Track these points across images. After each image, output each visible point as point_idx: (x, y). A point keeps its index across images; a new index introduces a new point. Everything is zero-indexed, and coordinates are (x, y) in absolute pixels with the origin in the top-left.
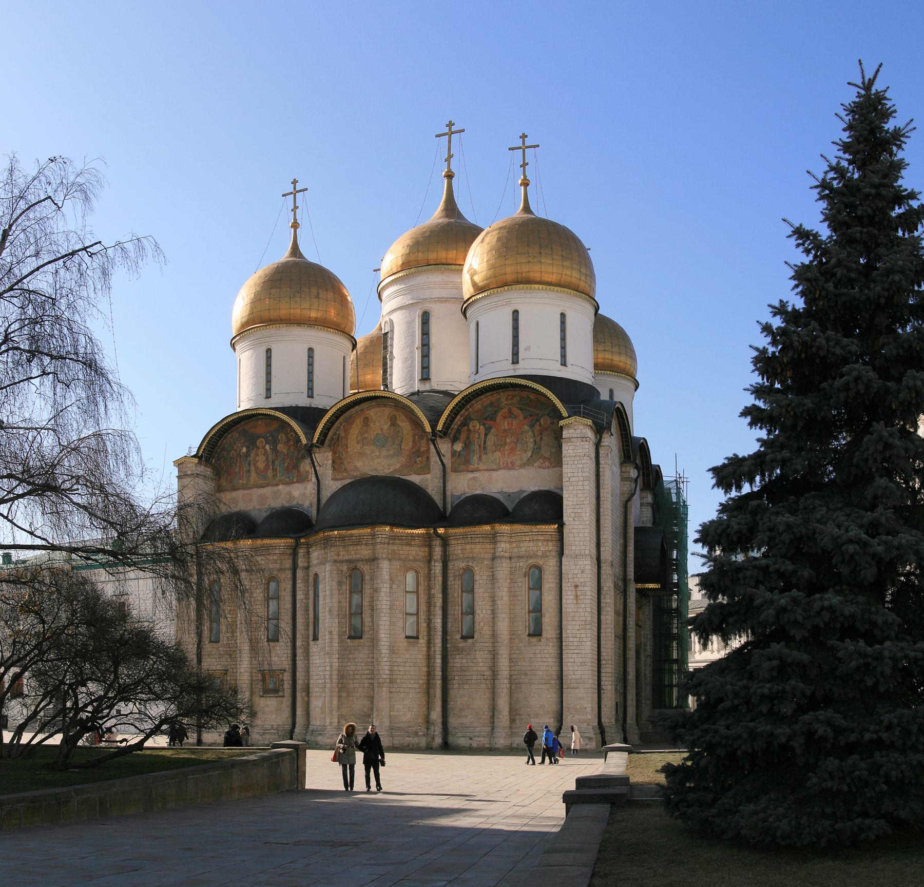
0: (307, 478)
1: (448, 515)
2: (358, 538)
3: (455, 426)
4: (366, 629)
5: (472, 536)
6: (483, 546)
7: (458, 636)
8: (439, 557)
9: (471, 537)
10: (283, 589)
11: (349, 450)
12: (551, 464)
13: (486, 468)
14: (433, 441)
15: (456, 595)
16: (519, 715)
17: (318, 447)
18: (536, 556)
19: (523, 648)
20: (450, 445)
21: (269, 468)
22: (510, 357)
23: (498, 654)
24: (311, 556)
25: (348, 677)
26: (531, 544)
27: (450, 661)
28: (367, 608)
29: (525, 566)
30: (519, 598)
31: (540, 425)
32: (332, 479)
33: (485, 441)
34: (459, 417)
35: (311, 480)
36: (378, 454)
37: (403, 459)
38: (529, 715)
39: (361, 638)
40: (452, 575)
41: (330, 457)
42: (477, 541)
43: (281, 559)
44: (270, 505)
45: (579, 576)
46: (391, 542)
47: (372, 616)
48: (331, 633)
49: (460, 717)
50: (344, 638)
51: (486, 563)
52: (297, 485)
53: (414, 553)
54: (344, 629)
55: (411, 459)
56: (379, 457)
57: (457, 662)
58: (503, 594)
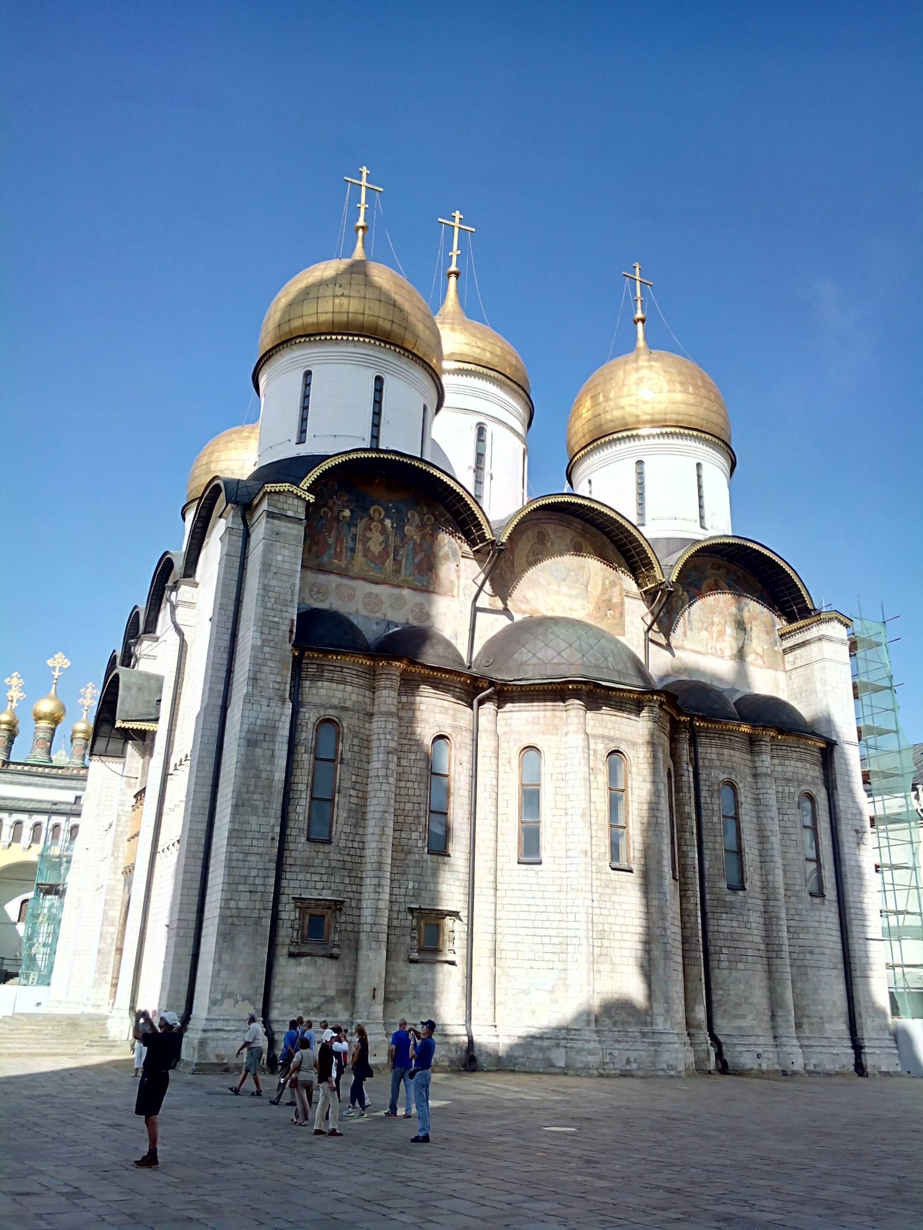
0: (452, 591)
5: (731, 738)
7: (724, 885)
10: (458, 763)
12: (764, 663)
13: (692, 648)
15: (715, 819)
16: (808, 1017)
18: (808, 783)
19: (805, 913)
21: (388, 557)
23: (778, 918)
25: (611, 937)
26: (799, 764)
27: (711, 922)
29: (797, 794)
30: (793, 837)
31: (749, 609)
36: (556, 588)
37: (591, 607)
38: (821, 1018)
40: (707, 788)
44: (385, 615)
49: (737, 1017)
51: (749, 779)
55: (600, 609)
57: (724, 924)
58: (774, 826)
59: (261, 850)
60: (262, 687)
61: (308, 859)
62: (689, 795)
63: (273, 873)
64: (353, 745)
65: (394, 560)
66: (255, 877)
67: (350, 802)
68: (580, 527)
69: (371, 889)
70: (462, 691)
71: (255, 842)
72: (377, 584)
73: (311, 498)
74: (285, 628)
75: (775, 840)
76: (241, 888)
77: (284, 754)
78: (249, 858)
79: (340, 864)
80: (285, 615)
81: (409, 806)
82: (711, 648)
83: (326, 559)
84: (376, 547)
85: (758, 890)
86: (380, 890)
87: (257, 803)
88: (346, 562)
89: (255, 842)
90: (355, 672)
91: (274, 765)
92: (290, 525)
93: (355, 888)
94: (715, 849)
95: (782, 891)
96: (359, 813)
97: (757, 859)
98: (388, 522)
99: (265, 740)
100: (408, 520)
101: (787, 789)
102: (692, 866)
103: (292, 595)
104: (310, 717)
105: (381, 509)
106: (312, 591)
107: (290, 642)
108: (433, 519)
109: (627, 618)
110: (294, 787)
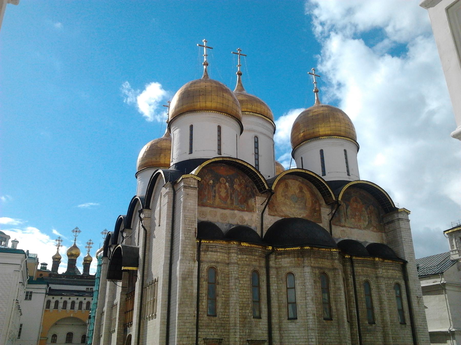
0: (254, 210)
4: (334, 314)
7: (367, 322)
10: (262, 281)
11: (277, 199)
12: (377, 230)
15: (362, 296)
19: (399, 331)
26: (393, 271)
27: (363, 337)
28: (332, 299)
29: (393, 283)
30: (393, 301)
33: (346, 212)
36: (294, 205)
37: (307, 212)
39: (332, 320)
43: (259, 260)
45: (418, 291)
47: (336, 305)
48: (314, 314)
50: (321, 318)
51: (374, 279)
52: (247, 213)
54: (321, 313)
56: (294, 207)
58: (385, 297)
59: (190, 321)
60: (186, 256)
61: (208, 323)
62: (351, 287)
63: (195, 330)
64: (222, 277)
66: (188, 331)
67: (222, 300)
69: (233, 333)
71: (188, 318)
73: (199, 179)
74: (193, 232)
75: (386, 303)
76: (184, 336)
77: (196, 282)
78: (186, 324)
79: (220, 325)
80: (193, 226)
81: (244, 300)
82: (356, 225)
83: (205, 201)
84: (223, 194)
85: (380, 323)
86: (236, 334)
87: (188, 302)
88: (212, 202)
89: (188, 318)
90: (220, 247)
91: (193, 286)
92: (192, 190)
93: (226, 333)
94: (363, 308)
95: (389, 323)
96: (226, 304)
97: (379, 311)
98: (227, 184)
99: (189, 277)
100: (235, 183)
101: (389, 282)
102: (354, 316)
103: (195, 218)
104: (205, 266)
105: (224, 179)
106: (200, 214)
107: (195, 237)
108: (244, 181)
109: (322, 216)
110: (200, 295)
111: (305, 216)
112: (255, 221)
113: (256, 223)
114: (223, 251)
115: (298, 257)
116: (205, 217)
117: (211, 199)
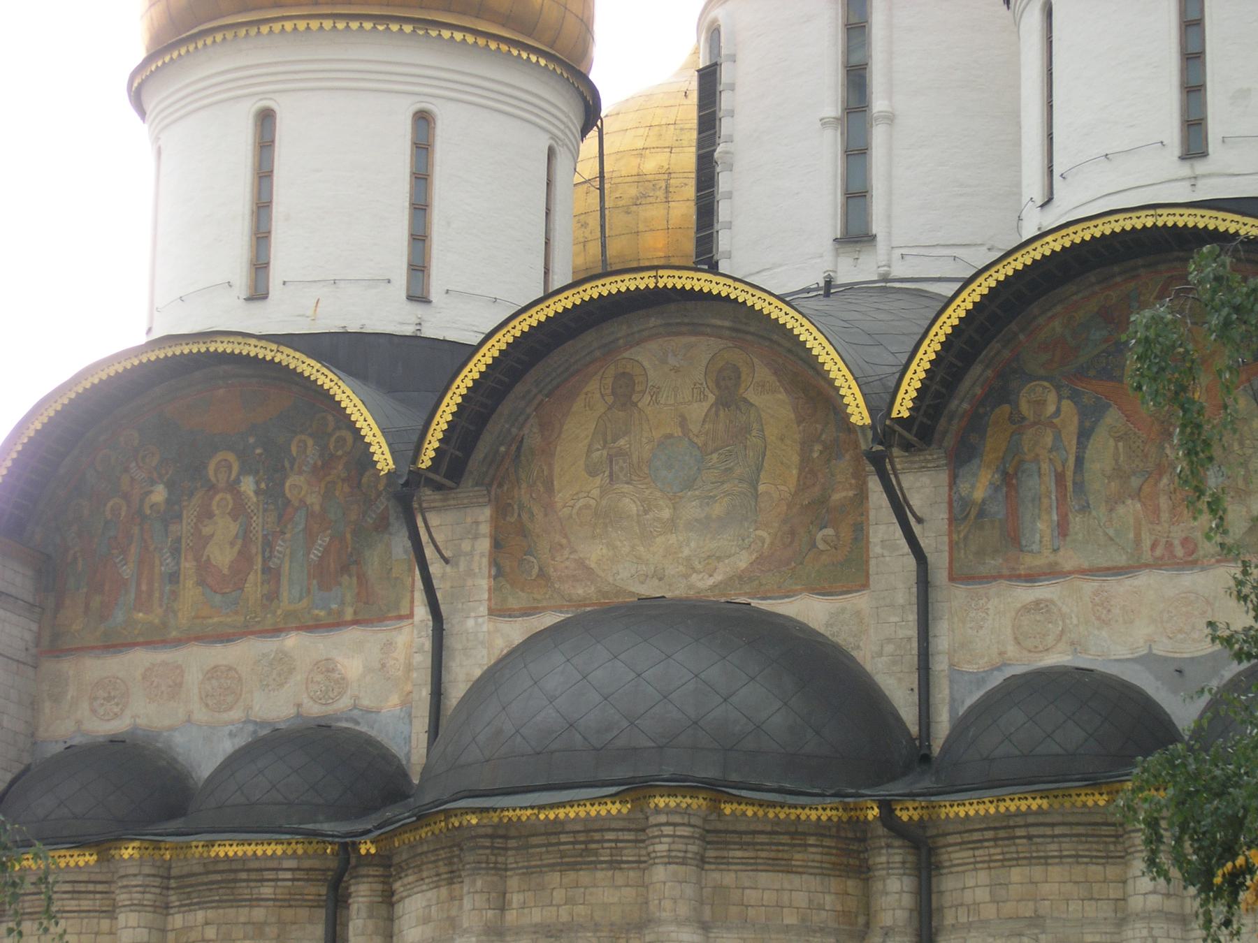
1: (936, 750)
2: (582, 837)
3: (960, 404)
6: (1078, 871)
8: (901, 915)
9: (1030, 837)
11: (559, 498)
13: (1086, 565)
14: (879, 462)
17: (439, 487)
20: (944, 477)
22: (1171, 131)
24: (399, 909)
32: (491, 612)
33: (1079, 461)
34: (976, 370)
35: (411, 616)
36: (666, 514)
41: (485, 529)
42: (1052, 849)
46: (711, 853)
52: (352, 634)
53: (801, 899)
55: (793, 533)
56: (671, 525)
65: (263, 572)
68: (727, 324)
70: (299, 875)
72: (225, 638)
82: (1154, 546)
83: (120, 616)
84: (222, 556)
98: (248, 485)
105: (231, 457)
106: (95, 699)
111: (743, 565)
112: (400, 673)
113: (409, 687)
114: (86, 904)
115: (450, 882)
116: (116, 710)
117: (157, 595)
